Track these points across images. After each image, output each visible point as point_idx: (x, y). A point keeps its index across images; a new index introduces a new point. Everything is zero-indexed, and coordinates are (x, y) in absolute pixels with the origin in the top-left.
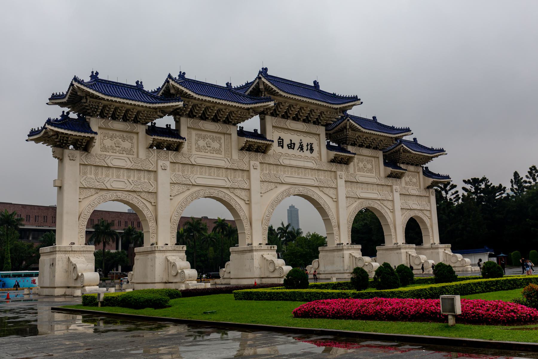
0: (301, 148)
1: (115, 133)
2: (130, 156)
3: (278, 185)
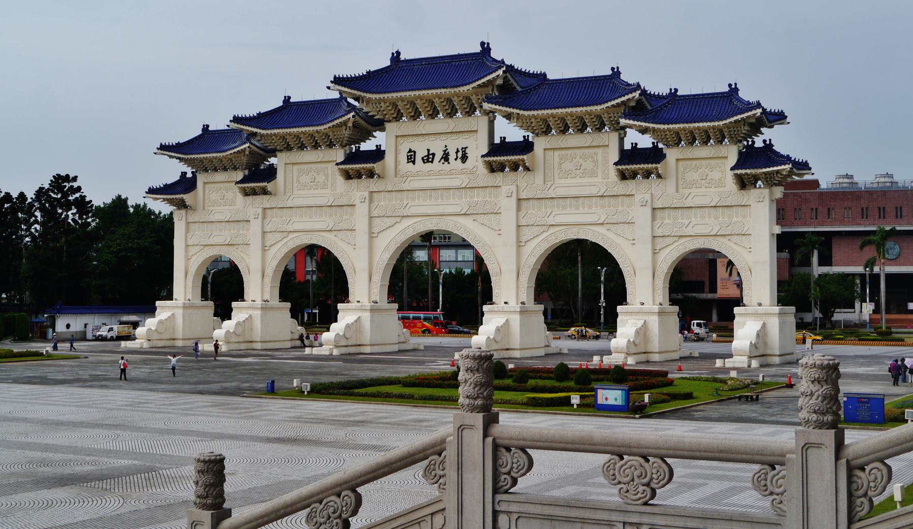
0: (446, 157)
1: (219, 185)
2: (232, 207)
3: (398, 219)
